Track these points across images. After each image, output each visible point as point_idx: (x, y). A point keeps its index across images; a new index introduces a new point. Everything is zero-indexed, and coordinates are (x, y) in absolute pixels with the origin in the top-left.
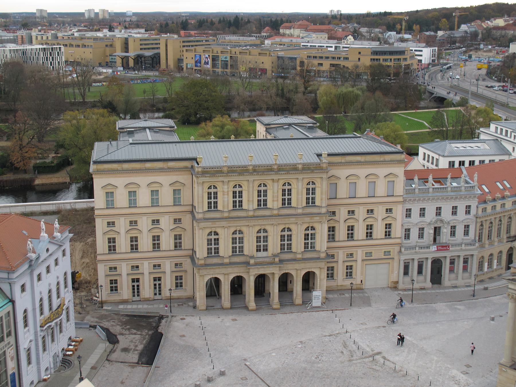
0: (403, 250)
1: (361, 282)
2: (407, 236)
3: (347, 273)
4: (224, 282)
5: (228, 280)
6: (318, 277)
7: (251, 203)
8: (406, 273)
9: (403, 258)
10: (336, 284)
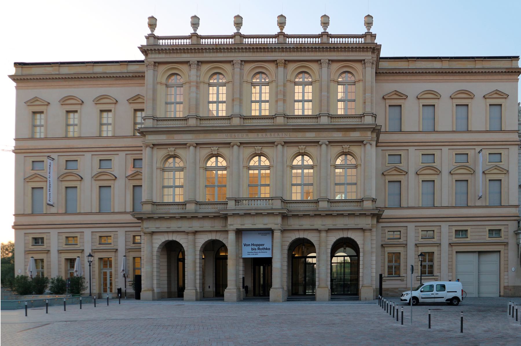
7: (237, 103)
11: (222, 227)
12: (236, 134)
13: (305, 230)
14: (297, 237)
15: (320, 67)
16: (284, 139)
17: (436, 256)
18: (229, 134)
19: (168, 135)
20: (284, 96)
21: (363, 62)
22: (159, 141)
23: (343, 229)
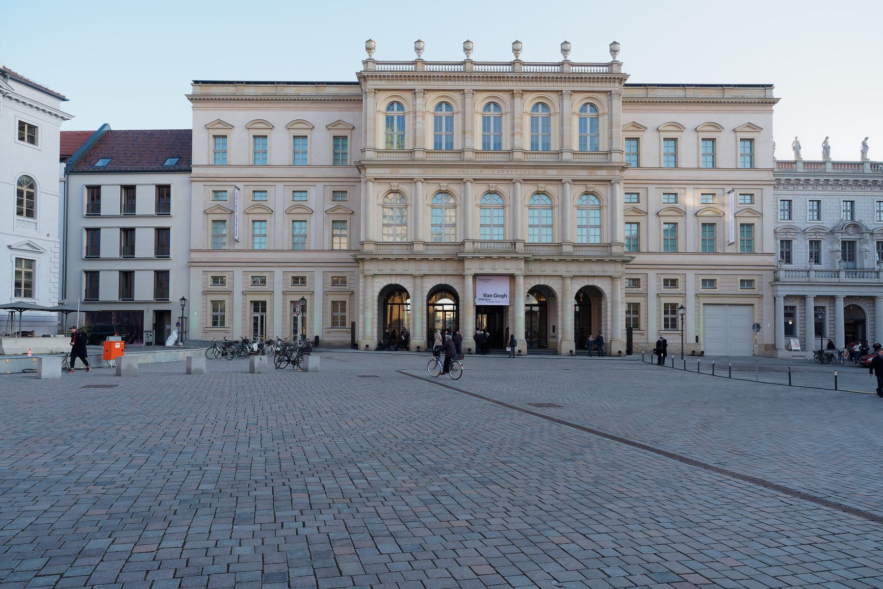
0: (782, 275)
1: (697, 341)
2: (787, 257)
3: (666, 320)
5: (422, 292)
6: (609, 300)
8: (790, 331)
9: (783, 291)
10: (645, 341)
11: (455, 270)
12: (469, 170)
14: (537, 283)
15: (561, 99)
16: (523, 176)
18: (461, 170)
19: (391, 169)
20: (521, 129)
21: (609, 93)
22: (382, 175)
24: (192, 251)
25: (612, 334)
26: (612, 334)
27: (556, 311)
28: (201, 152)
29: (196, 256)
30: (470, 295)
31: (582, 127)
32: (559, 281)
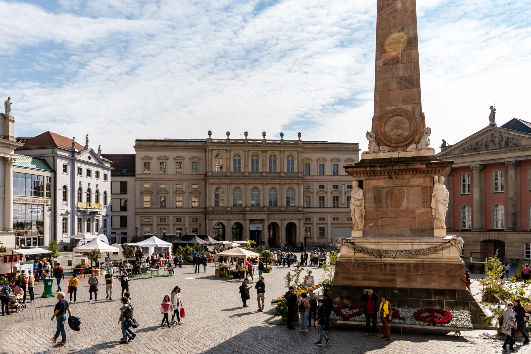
4: (227, 227)
5: (230, 225)
6: (298, 227)
13: (275, 219)
17: (325, 229)
20: (266, 164)
23: (290, 219)
24: (136, 208)
25: (299, 240)
26: (299, 240)
27: (279, 232)
28: (139, 168)
29: (138, 210)
30: (248, 227)
31: (288, 164)
32: (280, 221)
